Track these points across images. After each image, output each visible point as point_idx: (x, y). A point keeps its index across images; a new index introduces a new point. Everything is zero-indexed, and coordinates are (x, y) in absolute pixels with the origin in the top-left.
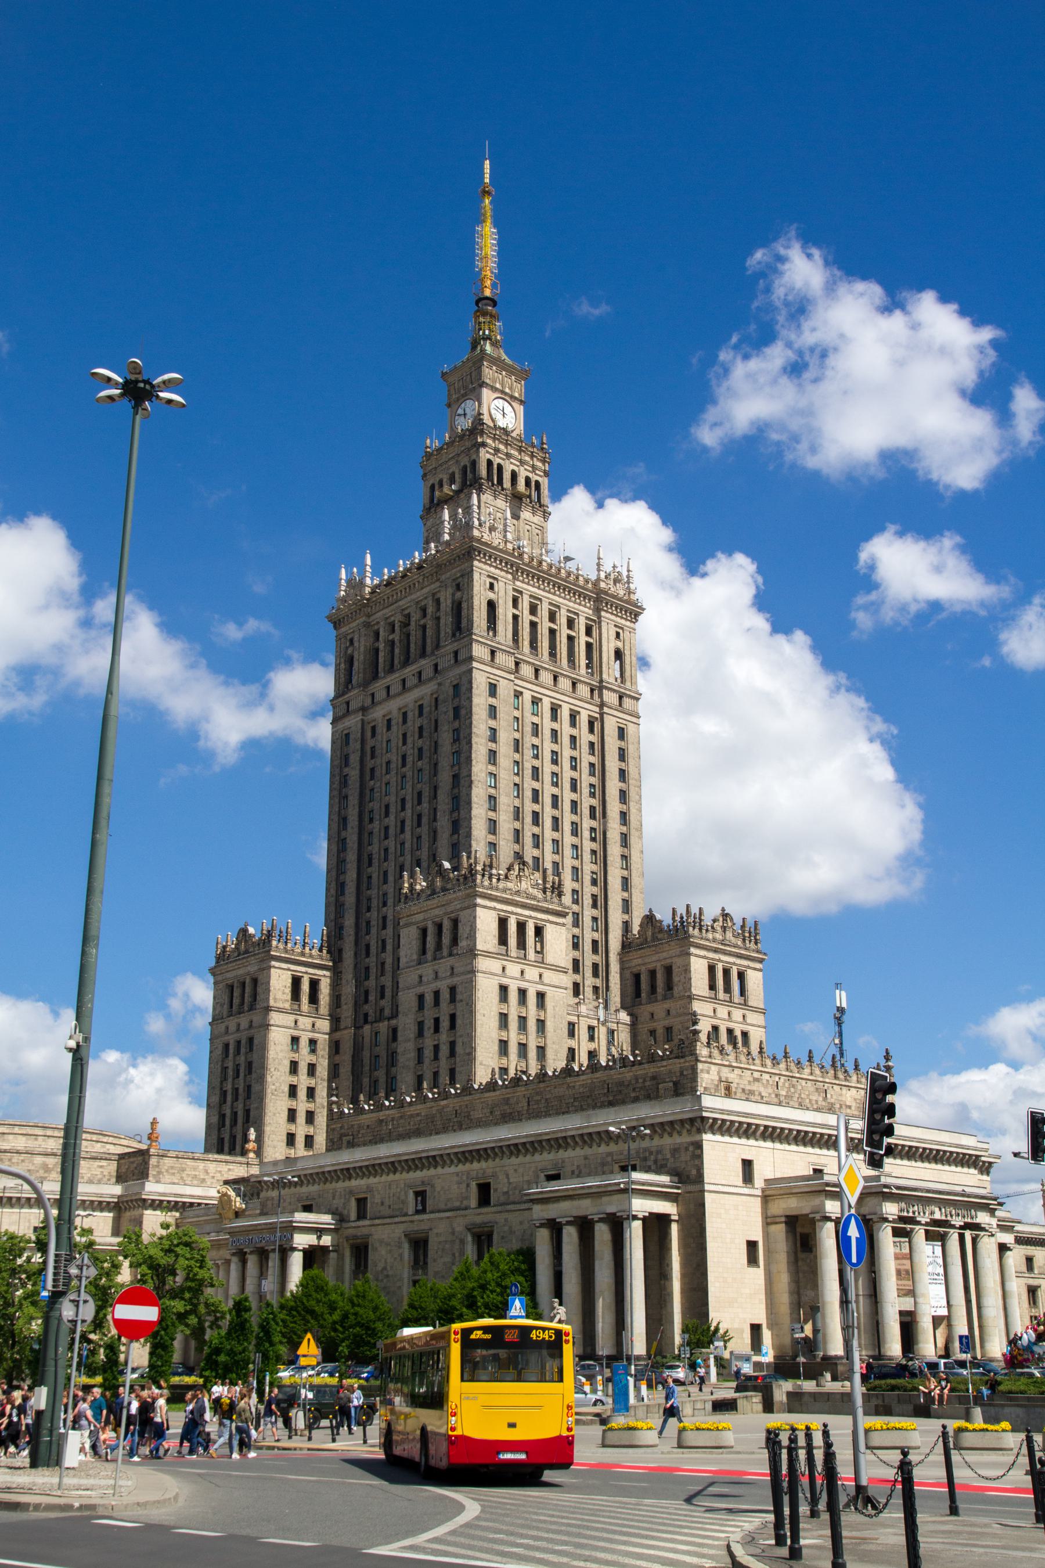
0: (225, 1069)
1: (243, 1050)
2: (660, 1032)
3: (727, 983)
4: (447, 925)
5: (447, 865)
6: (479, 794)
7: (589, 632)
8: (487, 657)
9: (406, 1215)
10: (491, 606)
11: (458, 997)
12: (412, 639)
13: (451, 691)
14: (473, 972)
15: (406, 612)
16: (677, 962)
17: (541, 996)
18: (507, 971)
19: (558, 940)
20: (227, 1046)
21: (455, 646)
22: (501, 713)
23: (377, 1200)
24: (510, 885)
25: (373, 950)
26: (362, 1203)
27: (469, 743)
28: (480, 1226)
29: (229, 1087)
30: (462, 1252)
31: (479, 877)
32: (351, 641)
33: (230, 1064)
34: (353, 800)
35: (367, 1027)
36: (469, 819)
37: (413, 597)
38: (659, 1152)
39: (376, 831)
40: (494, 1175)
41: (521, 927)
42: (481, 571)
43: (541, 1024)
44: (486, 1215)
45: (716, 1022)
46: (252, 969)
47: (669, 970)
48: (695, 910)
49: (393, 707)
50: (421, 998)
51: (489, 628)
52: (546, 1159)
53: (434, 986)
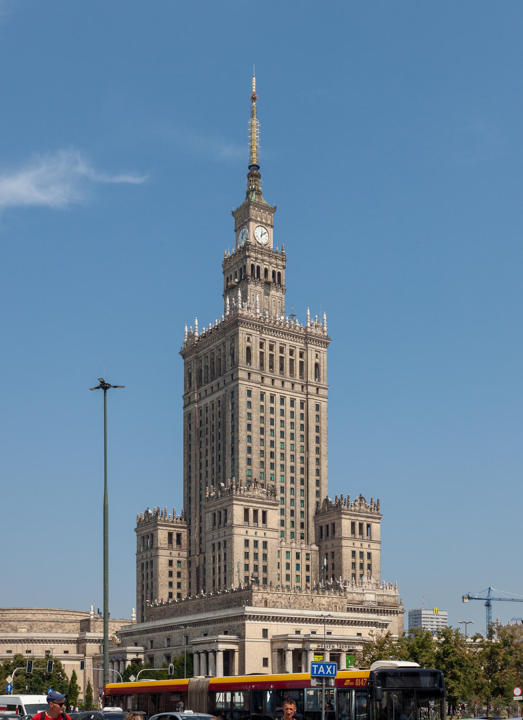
3: (361, 530)
4: (223, 512)
5: (222, 485)
6: (242, 447)
7: (301, 356)
8: (246, 377)
12: (215, 366)
15: (213, 352)
18: (249, 533)
19: (274, 517)
22: (253, 405)
24: (250, 493)
27: (238, 421)
31: (234, 491)
37: (215, 344)
38: (234, 627)
41: (256, 512)
43: (265, 556)
50: (214, 545)
53: (218, 540)
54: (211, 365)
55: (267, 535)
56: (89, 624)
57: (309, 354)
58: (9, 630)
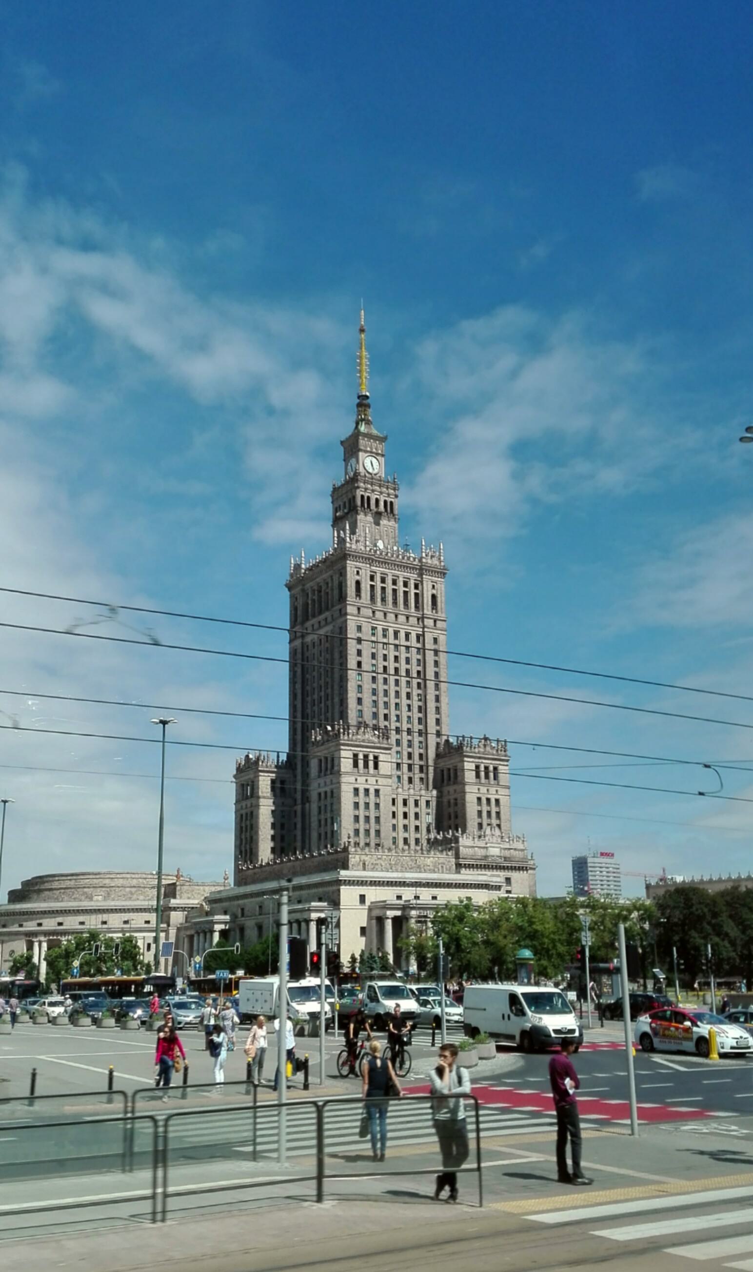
0: (241, 828)
2: (452, 801)
5: (329, 728)
7: (416, 587)
8: (355, 612)
10: (358, 583)
16: (459, 765)
17: (377, 791)
20: (242, 815)
26: (243, 910)
33: (244, 825)
34: (298, 686)
36: (347, 699)
42: (351, 566)
43: (377, 805)
45: (479, 795)
46: (252, 776)
50: (320, 794)
51: (357, 596)
54: (318, 598)
55: (379, 783)
56: (175, 889)
57: (425, 585)
58: (83, 898)
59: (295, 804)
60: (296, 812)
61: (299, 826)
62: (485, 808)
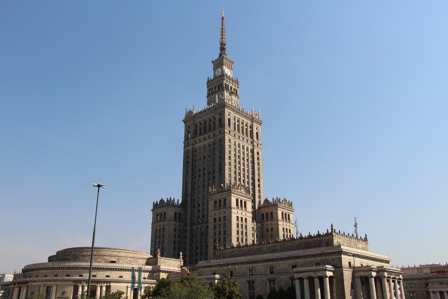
0: (156, 236)
1: (161, 231)
2: (269, 230)
4: (222, 201)
5: (222, 185)
9: (247, 276)
10: (229, 120)
11: (226, 219)
12: (207, 127)
13: (219, 141)
14: (231, 212)
16: (275, 211)
17: (246, 219)
20: (156, 230)
21: (220, 129)
23: (237, 271)
24: (239, 191)
25: (196, 206)
28: (271, 279)
29: (157, 240)
30: (266, 286)
32: (189, 127)
33: (158, 235)
34: (190, 168)
35: (195, 226)
38: (328, 260)
39: (197, 176)
40: (275, 266)
41: (241, 201)
42: (227, 111)
43: (246, 226)
44: (273, 276)
45: (284, 227)
47: (272, 213)
48: (278, 198)
49: (202, 144)
52: (292, 262)
53: (219, 216)
59: (186, 226)
60: (186, 230)
61: (188, 237)
62: (286, 233)
